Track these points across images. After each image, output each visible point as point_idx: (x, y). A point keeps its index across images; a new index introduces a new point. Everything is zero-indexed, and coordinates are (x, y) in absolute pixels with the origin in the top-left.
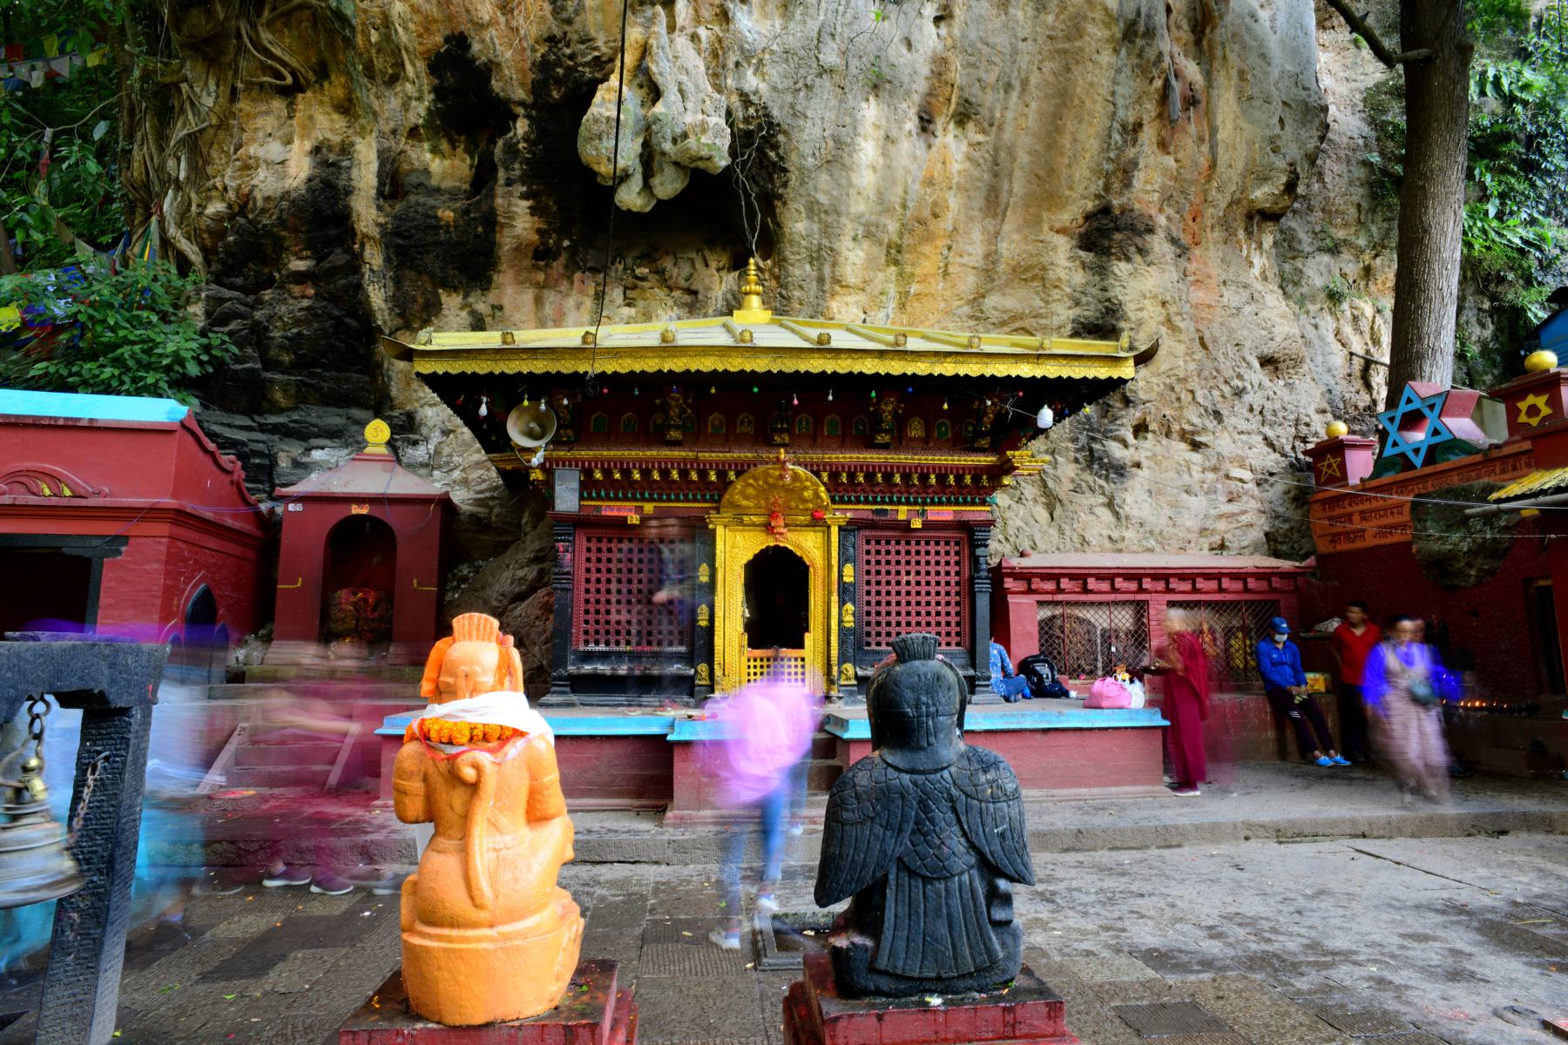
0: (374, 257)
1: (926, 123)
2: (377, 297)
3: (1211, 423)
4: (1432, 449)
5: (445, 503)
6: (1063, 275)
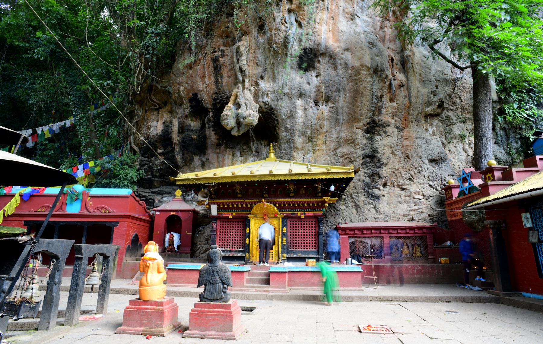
0: (177, 148)
1: (316, 103)
2: (178, 158)
3: (408, 182)
4: (469, 188)
5: (194, 212)
6: (360, 142)
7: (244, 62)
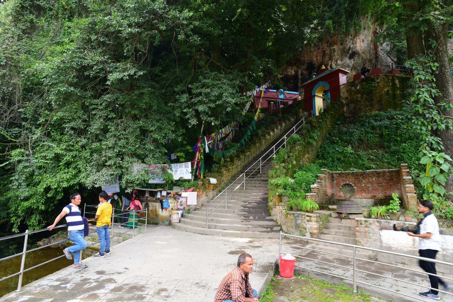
7: (336, 54)
